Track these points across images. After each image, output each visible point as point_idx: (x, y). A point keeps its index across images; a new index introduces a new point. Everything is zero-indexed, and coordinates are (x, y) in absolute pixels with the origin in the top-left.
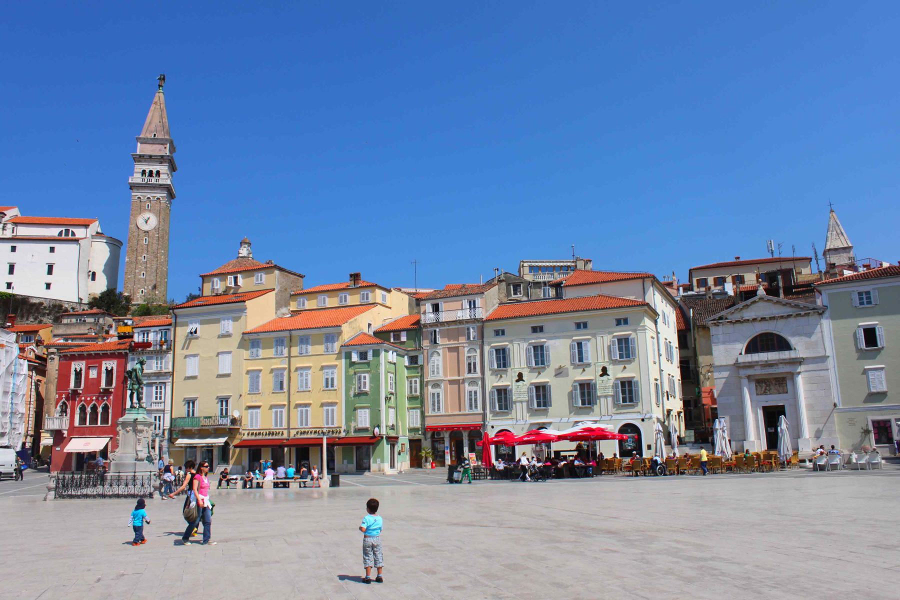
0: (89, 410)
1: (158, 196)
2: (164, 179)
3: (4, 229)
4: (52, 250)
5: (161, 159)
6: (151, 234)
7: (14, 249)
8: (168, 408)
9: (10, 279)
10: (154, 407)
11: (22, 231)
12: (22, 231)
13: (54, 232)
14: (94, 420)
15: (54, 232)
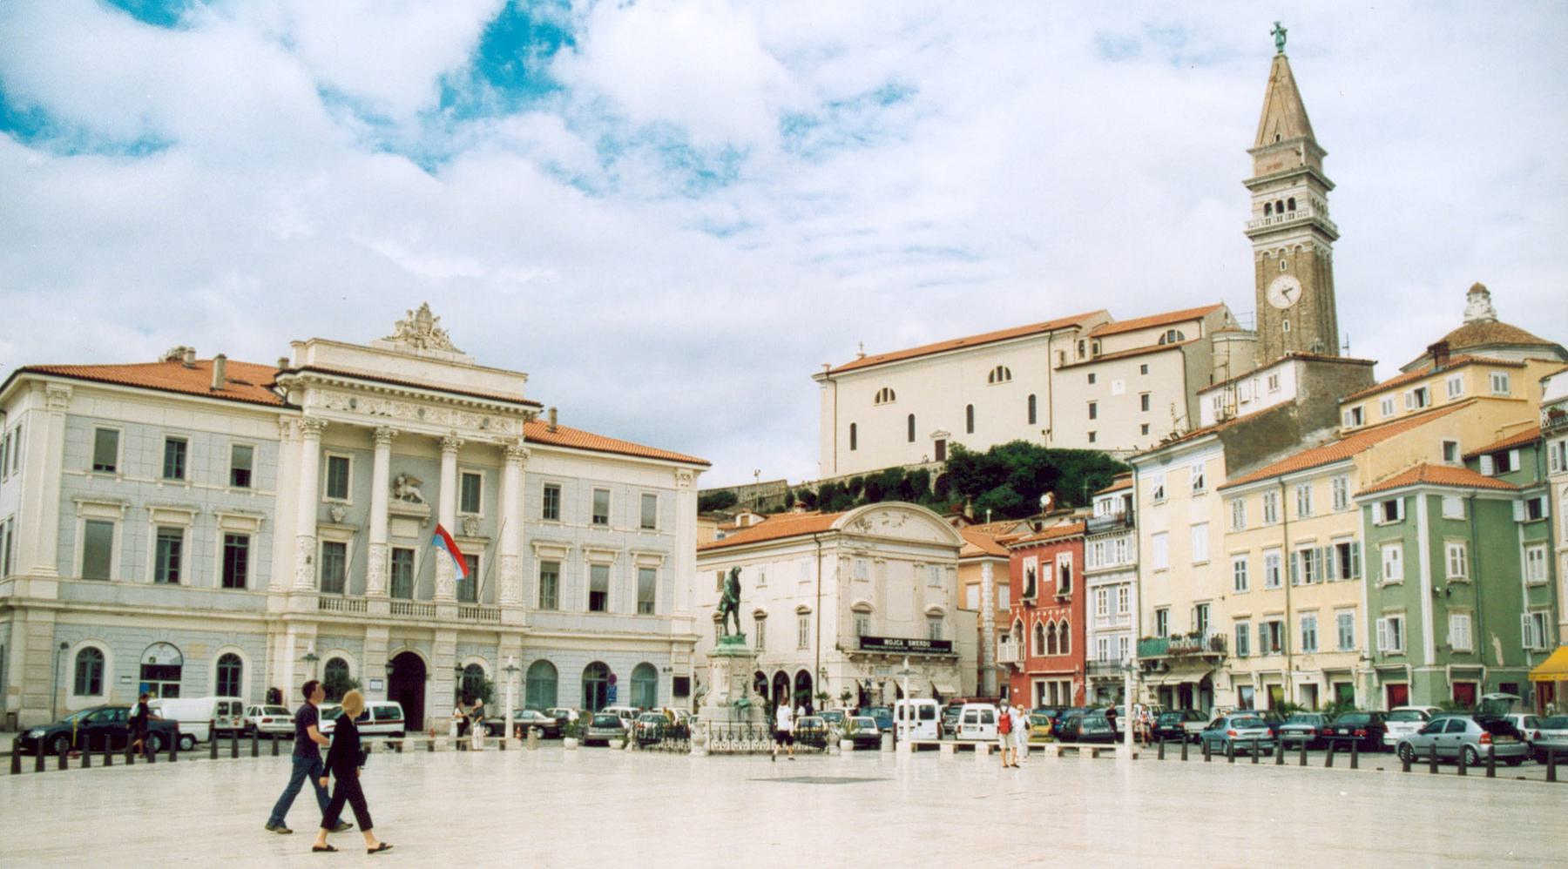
0: (1045, 631)
1: (1297, 242)
2: (1305, 211)
3: (1082, 352)
4: (1144, 369)
5: (1293, 179)
6: (1293, 313)
7: (1092, 378)
8: (1134, 625)
9: (1092, 425)
10: (1120, 624)
11: (1110, 346)
12: (1110, 346)
13: (1151, 339)
14: (1052, 649)
15: (1151, 339)
